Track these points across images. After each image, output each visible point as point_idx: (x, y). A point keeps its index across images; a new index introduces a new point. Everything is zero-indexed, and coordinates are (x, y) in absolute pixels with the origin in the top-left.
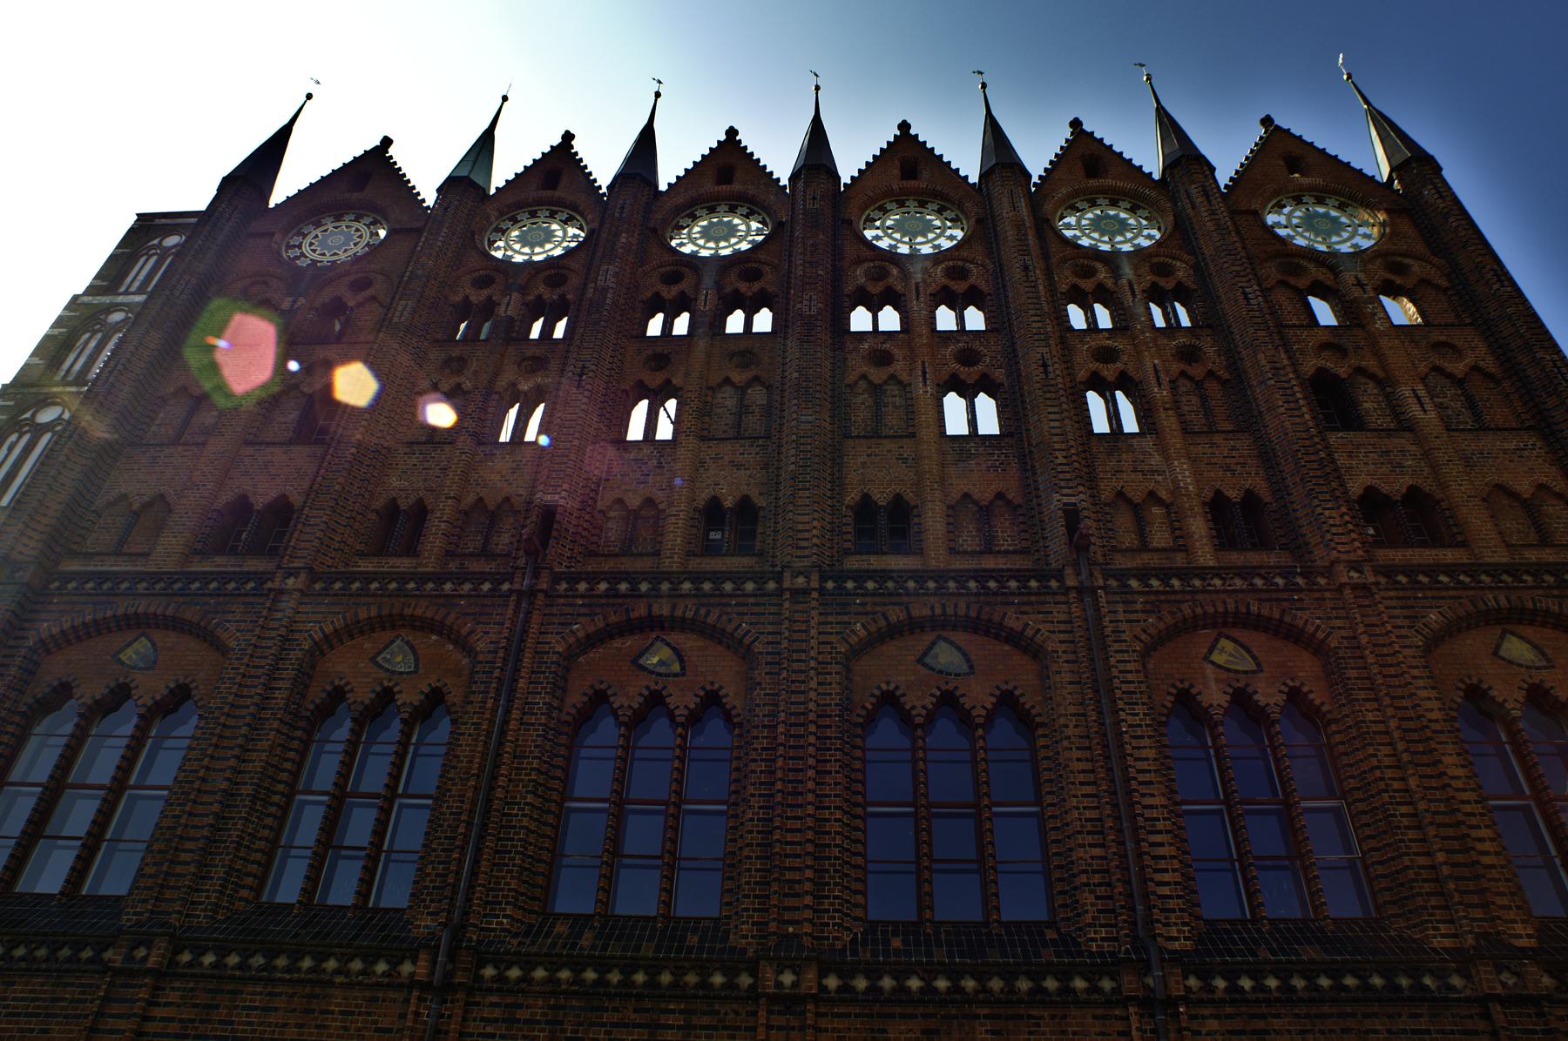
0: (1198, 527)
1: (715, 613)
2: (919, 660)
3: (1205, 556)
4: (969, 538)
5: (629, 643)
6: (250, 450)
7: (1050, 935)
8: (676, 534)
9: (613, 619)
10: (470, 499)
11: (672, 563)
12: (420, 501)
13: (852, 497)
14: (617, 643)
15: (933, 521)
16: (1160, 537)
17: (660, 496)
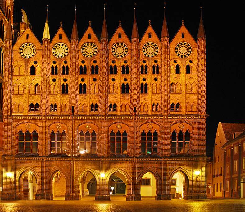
0: (150, 109)
1: (94, 121)
2: (116, 127)
3: (150, 113)
4: (123, 110)
5: (85, 124)
6: (29, 95)
7: (127, 155)
8: (88, 109)
9: (82, 122)
10: (61, 104)
11: (88, 114)
12: (55, 104)
13: (109, 104)
14: (83, 124)
15: (118, 107)
16: (146, 110)
17: (86, 103)
